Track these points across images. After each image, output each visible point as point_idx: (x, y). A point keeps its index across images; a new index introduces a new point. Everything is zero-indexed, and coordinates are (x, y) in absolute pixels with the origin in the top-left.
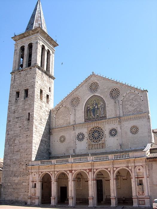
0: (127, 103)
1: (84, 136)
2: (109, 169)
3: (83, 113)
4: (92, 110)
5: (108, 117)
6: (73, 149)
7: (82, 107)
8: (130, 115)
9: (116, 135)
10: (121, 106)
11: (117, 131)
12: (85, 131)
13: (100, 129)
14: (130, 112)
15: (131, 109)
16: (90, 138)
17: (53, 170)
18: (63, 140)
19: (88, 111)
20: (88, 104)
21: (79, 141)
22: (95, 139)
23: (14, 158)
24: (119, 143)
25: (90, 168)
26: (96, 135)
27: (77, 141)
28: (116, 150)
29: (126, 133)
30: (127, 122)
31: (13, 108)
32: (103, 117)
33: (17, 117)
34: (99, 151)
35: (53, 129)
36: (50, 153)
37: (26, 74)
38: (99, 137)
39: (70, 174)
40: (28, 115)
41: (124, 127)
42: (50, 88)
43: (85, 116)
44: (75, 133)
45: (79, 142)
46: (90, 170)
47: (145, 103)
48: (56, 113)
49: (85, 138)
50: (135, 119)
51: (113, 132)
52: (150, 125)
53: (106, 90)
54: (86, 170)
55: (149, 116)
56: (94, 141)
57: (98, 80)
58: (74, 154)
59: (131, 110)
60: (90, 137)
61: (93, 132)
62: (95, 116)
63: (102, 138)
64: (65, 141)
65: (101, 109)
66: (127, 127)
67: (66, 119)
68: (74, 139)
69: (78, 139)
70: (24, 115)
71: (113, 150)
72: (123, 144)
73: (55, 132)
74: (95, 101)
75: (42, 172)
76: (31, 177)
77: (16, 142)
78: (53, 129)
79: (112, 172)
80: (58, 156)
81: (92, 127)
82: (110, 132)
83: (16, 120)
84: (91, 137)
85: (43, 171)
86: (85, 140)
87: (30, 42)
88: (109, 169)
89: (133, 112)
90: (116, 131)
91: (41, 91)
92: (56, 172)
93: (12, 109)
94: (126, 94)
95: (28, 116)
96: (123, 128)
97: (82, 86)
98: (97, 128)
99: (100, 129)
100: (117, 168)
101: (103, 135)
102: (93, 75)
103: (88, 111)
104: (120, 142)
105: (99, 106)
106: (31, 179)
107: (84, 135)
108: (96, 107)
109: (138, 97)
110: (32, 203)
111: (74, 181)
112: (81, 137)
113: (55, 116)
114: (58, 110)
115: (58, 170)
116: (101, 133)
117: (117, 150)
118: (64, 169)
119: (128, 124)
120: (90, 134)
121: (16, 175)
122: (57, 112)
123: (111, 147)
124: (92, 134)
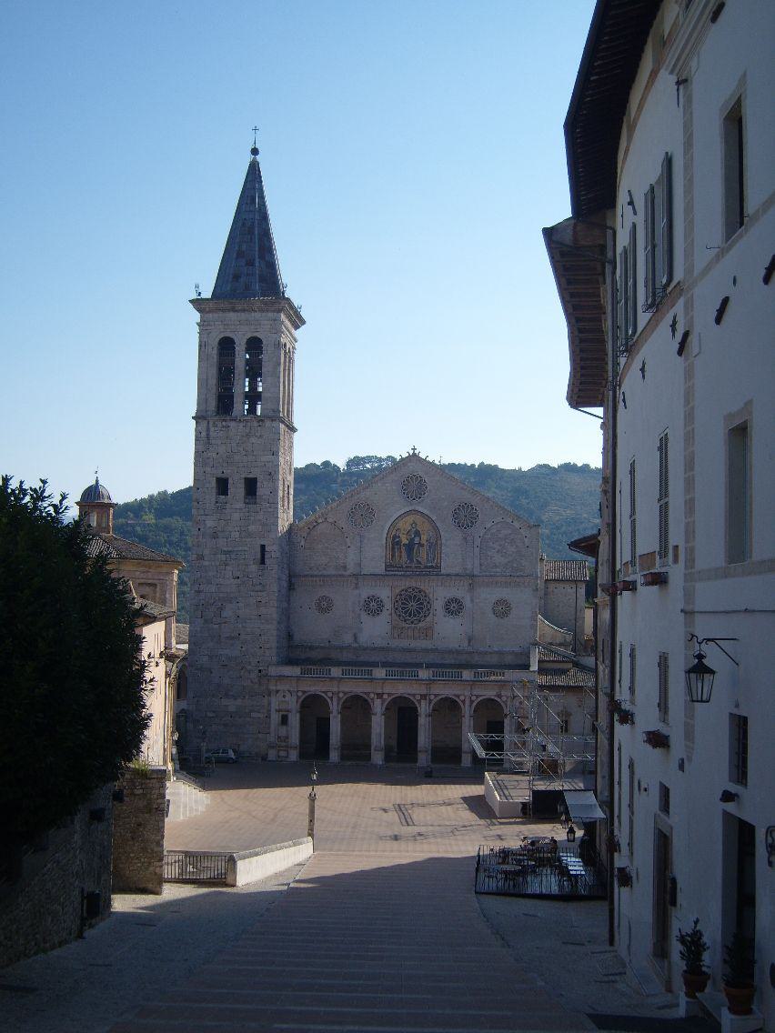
2: (462, 698)
10: (477, 550)
12: (385, 593)
14: (496, 566)
15: (498, 559)
17: (335, 689)
18: (324, 606)
23: (221, 652)
25: (425, 692)
26: (413, 605)
27: (364, 613)
31: (210, 523)
32: (432, 567)
33: (225, 549)
36: (290, 636)
37: (248, 435)
39: (378, 702)
40: (259, 549)
46: (424, 697)
49: (384, 609)
54: (414, 695)
56: (405, 621)
62: (412, 561)
65: (430, 547)
70: (246, 548)
75: (304, 692)
76: (275, 702)
77: (227, 613)
79: (467, 702)
83: (223, 557)
85: (306, 689)
86: (385, 617)
87: (255, 334)
88: (462, 698)
92: (341, 695)
93: (208, 525)
100: (477, 696)
102: (414, 454)
103: (395, 543)
105: (424, 538)
106: (275, 706)
108: (417, 540)
110: (279, 757)
111: (384, 715)
115: (346, 690)
117: (461, 648)
118: (361, 690)
121: (231, 693)
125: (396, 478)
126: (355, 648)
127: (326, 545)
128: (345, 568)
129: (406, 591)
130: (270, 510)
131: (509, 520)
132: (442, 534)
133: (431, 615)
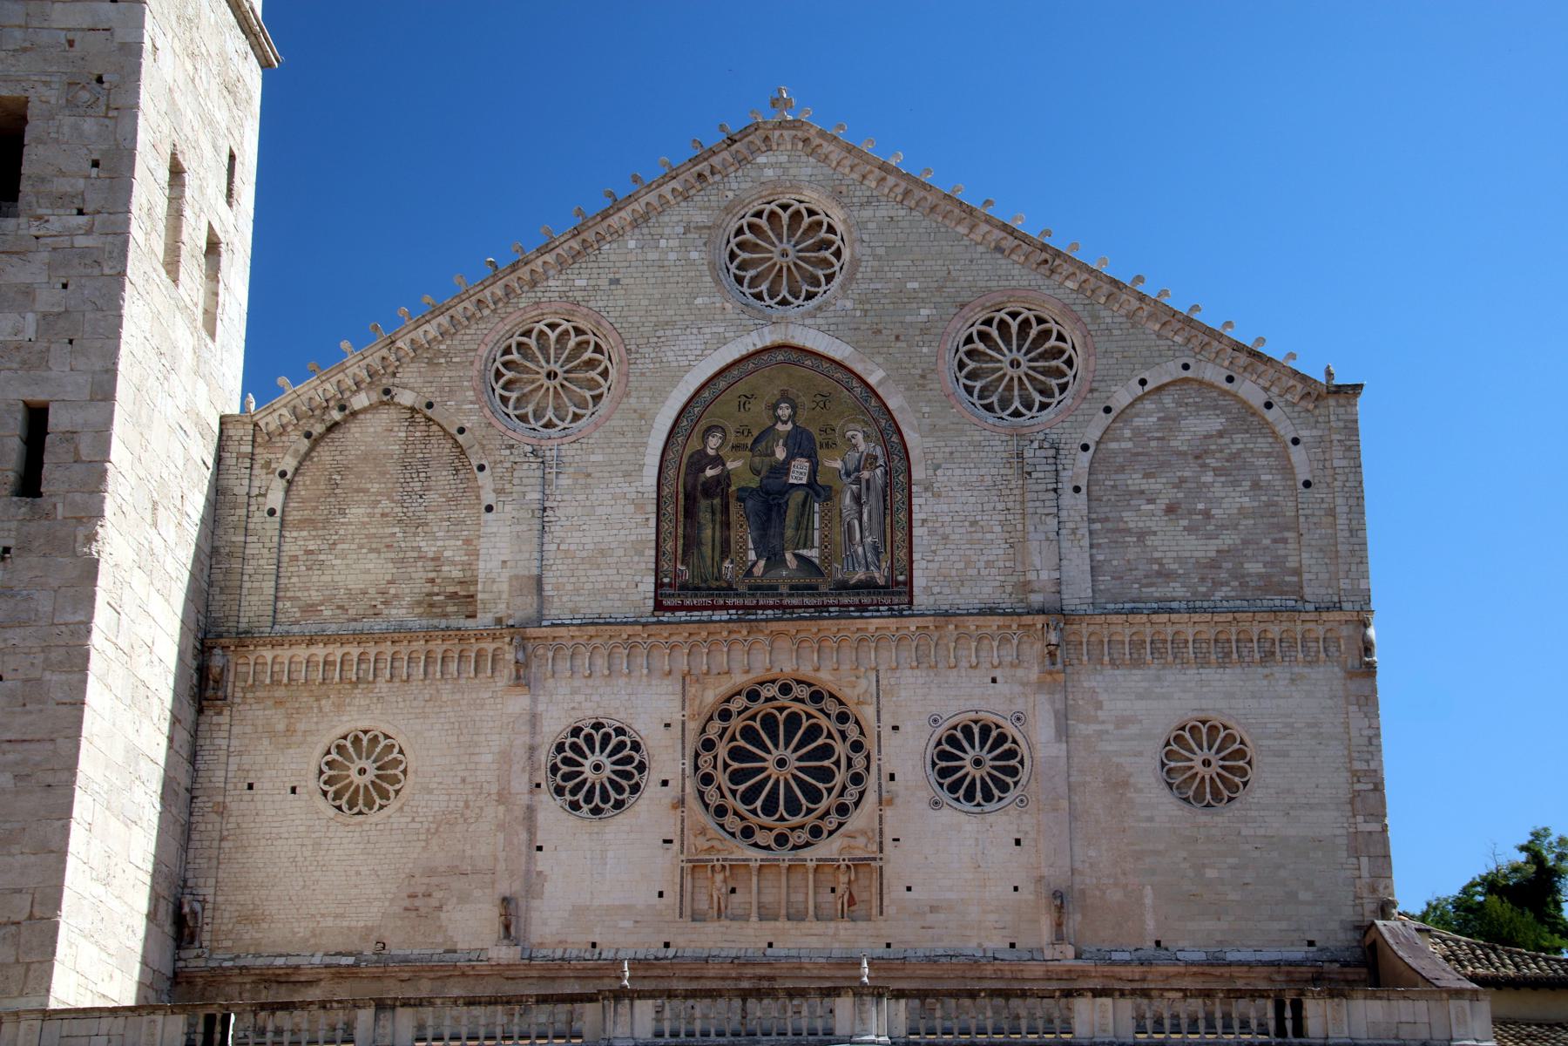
0: (1135, 481)
1: (641, 767)
3: (639, 507)
4: (744, 494)
5: (927, 590)
6: (504, 888)
7: (640, 446)
8: (1165, 608)
9: (1004, 788)
11: (1023, 749)
13: (834, 709)
14: (1166, 575)
16: (710, 790)
19: (704, 504)
20: (708, 431)
21: (575, 806)
22: (770, 808)
24: (1040, 879)
27: (551, 809)
28: (996, 943)
29: (1119, 785)
30: (1136, 679)
32: (869, 586)
34: (814, 942)
35: (245, 638)
38: (815, 796)
41: (1096, 720)
42: (232, 157)
43: (668, 546)
44: (534, 720)
45: (570, 820)
47: (1332, 513)
48: (289, 464)
50: (1224, 652)
51: (974, 763)
52: (1373, 739)
53: (924, 312)
55: (1368, 648)
56: (747, 833)
57: (838, 195)
58: (505, 954)
59: (1178, 560)
60: (707, 779)
61: (748, 733)
62: (774, 559)
63: (843, 810)
64: (394, 804)
65: (857, 499)
66: (1133, 729)
67: (430, 549)
68: (520, 784)
69: (559, 791)
71: (971, 946)
72: (1083, 892)
73: (275, 682)
74: (784, 411)
78: (245, 638)
80: (297, 967)
81: (739, 679)
82: (943, 755)
84: (722, 778)
89: (1203, 580)
90: (1011, 754)
91: (176, 172)
94: (1139, 391)
95: (14, 446)
96: (1091, 729)
97: (646, 217)
98: (797, 690)
99: (834, 709)
101: (857, 779)
104: (1045, 871)
107: (636, 747)
108: (799, 472)
109: (1263, 444)
112: (596, 767)
113: (275, 499)
114: (318, 429)
116: (841, 749)
119: (1140, 697)
120: (709, 745)
122: (307, 455)
123: (942, 916)
124: (736, 754)
125: (701, 218)
126: (504, 972)
127: (385, 503)
128: (467, 602)
129: (753, 696)
130: (81, 241)
131: (1213, 374)
132: (911, 438)
133: (871, 798)
